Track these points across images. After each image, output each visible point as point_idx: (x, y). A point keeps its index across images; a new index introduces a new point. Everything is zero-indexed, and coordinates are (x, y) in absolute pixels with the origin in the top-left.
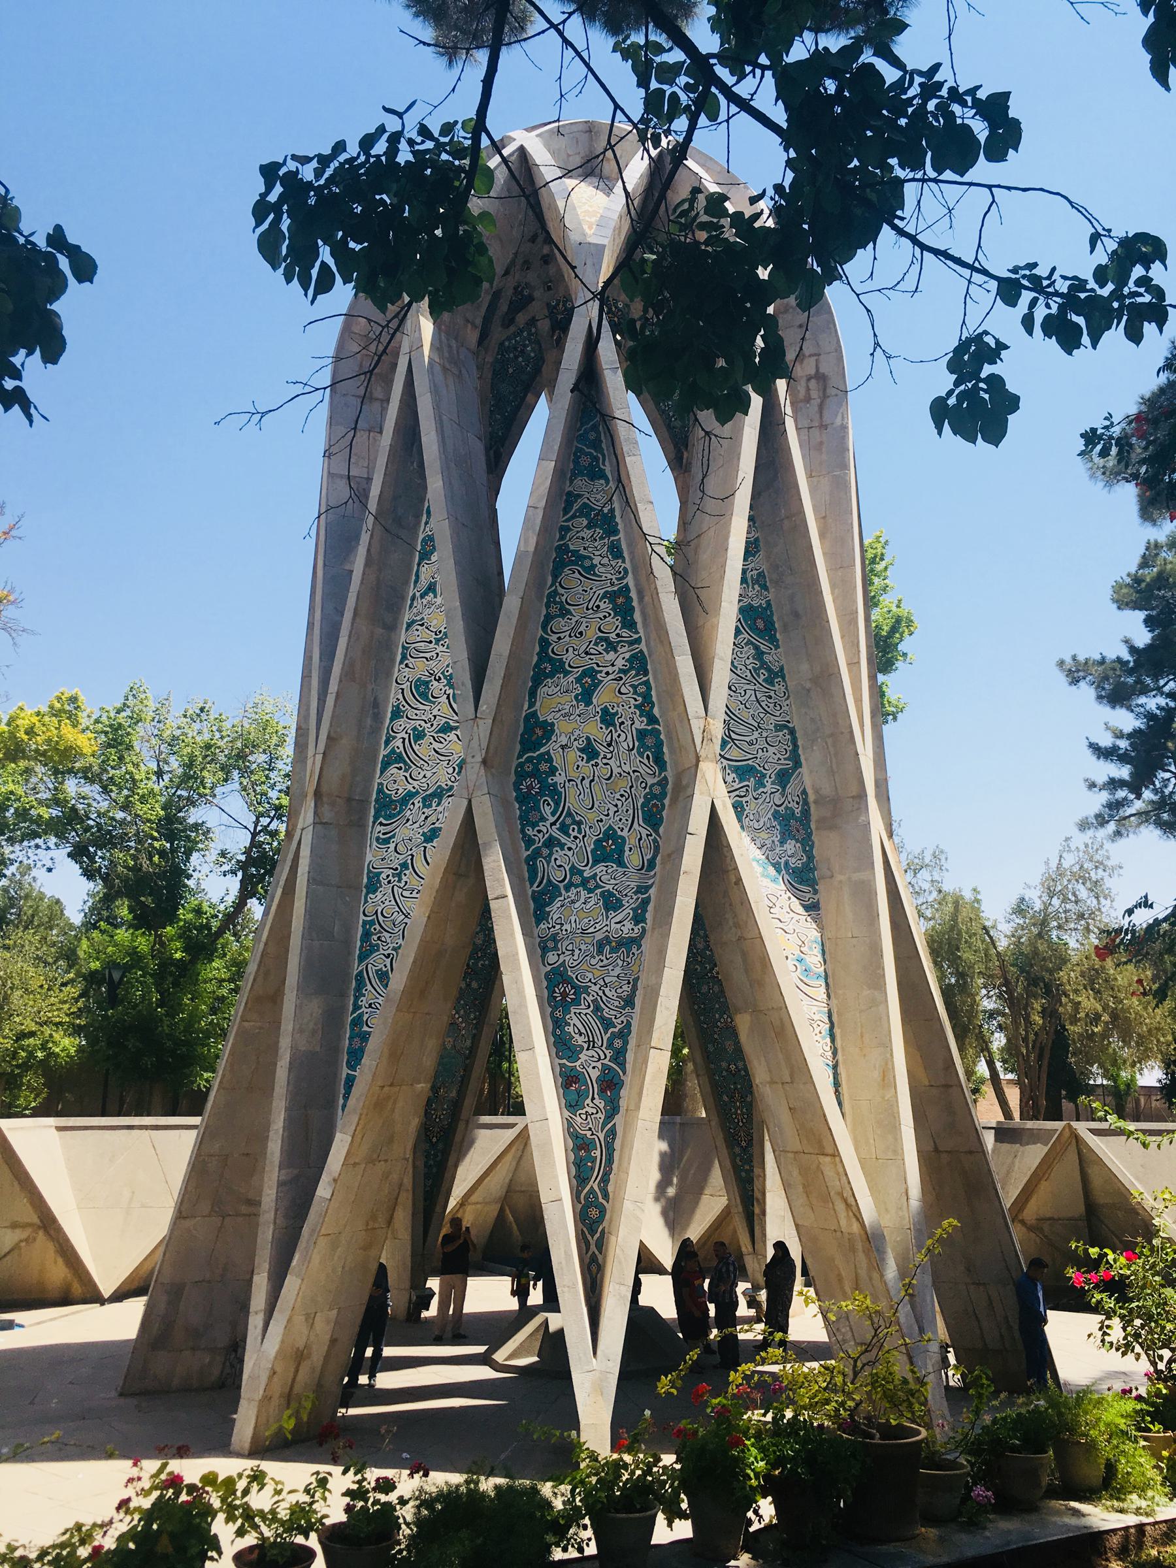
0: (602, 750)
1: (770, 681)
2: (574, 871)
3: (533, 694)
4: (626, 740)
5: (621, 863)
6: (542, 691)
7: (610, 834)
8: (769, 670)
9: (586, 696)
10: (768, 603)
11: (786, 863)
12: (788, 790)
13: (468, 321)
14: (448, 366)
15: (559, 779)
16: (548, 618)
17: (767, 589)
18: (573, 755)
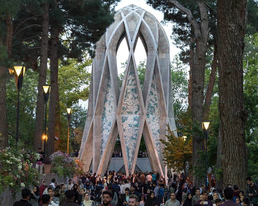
0: (111, 111)
1: (135, 99)
2: (106, 127)
3: (104, 104)
4: (113, 110)
5: (110, 126)
6: (105, 104)
7: (110, 122)
8: (135, 97)
9: (110, 104)
10: (136, 88)
11: (134, 124)
12: (137, 114)
13: (102, 49)
14: (98, 57)
15: (106, 115)
16: (106, 94)
17: (136, 86)
18: (108, 112)
